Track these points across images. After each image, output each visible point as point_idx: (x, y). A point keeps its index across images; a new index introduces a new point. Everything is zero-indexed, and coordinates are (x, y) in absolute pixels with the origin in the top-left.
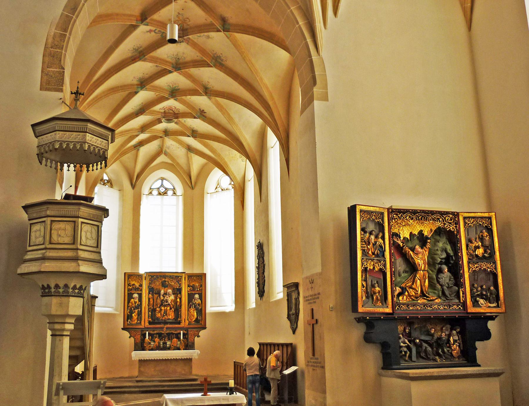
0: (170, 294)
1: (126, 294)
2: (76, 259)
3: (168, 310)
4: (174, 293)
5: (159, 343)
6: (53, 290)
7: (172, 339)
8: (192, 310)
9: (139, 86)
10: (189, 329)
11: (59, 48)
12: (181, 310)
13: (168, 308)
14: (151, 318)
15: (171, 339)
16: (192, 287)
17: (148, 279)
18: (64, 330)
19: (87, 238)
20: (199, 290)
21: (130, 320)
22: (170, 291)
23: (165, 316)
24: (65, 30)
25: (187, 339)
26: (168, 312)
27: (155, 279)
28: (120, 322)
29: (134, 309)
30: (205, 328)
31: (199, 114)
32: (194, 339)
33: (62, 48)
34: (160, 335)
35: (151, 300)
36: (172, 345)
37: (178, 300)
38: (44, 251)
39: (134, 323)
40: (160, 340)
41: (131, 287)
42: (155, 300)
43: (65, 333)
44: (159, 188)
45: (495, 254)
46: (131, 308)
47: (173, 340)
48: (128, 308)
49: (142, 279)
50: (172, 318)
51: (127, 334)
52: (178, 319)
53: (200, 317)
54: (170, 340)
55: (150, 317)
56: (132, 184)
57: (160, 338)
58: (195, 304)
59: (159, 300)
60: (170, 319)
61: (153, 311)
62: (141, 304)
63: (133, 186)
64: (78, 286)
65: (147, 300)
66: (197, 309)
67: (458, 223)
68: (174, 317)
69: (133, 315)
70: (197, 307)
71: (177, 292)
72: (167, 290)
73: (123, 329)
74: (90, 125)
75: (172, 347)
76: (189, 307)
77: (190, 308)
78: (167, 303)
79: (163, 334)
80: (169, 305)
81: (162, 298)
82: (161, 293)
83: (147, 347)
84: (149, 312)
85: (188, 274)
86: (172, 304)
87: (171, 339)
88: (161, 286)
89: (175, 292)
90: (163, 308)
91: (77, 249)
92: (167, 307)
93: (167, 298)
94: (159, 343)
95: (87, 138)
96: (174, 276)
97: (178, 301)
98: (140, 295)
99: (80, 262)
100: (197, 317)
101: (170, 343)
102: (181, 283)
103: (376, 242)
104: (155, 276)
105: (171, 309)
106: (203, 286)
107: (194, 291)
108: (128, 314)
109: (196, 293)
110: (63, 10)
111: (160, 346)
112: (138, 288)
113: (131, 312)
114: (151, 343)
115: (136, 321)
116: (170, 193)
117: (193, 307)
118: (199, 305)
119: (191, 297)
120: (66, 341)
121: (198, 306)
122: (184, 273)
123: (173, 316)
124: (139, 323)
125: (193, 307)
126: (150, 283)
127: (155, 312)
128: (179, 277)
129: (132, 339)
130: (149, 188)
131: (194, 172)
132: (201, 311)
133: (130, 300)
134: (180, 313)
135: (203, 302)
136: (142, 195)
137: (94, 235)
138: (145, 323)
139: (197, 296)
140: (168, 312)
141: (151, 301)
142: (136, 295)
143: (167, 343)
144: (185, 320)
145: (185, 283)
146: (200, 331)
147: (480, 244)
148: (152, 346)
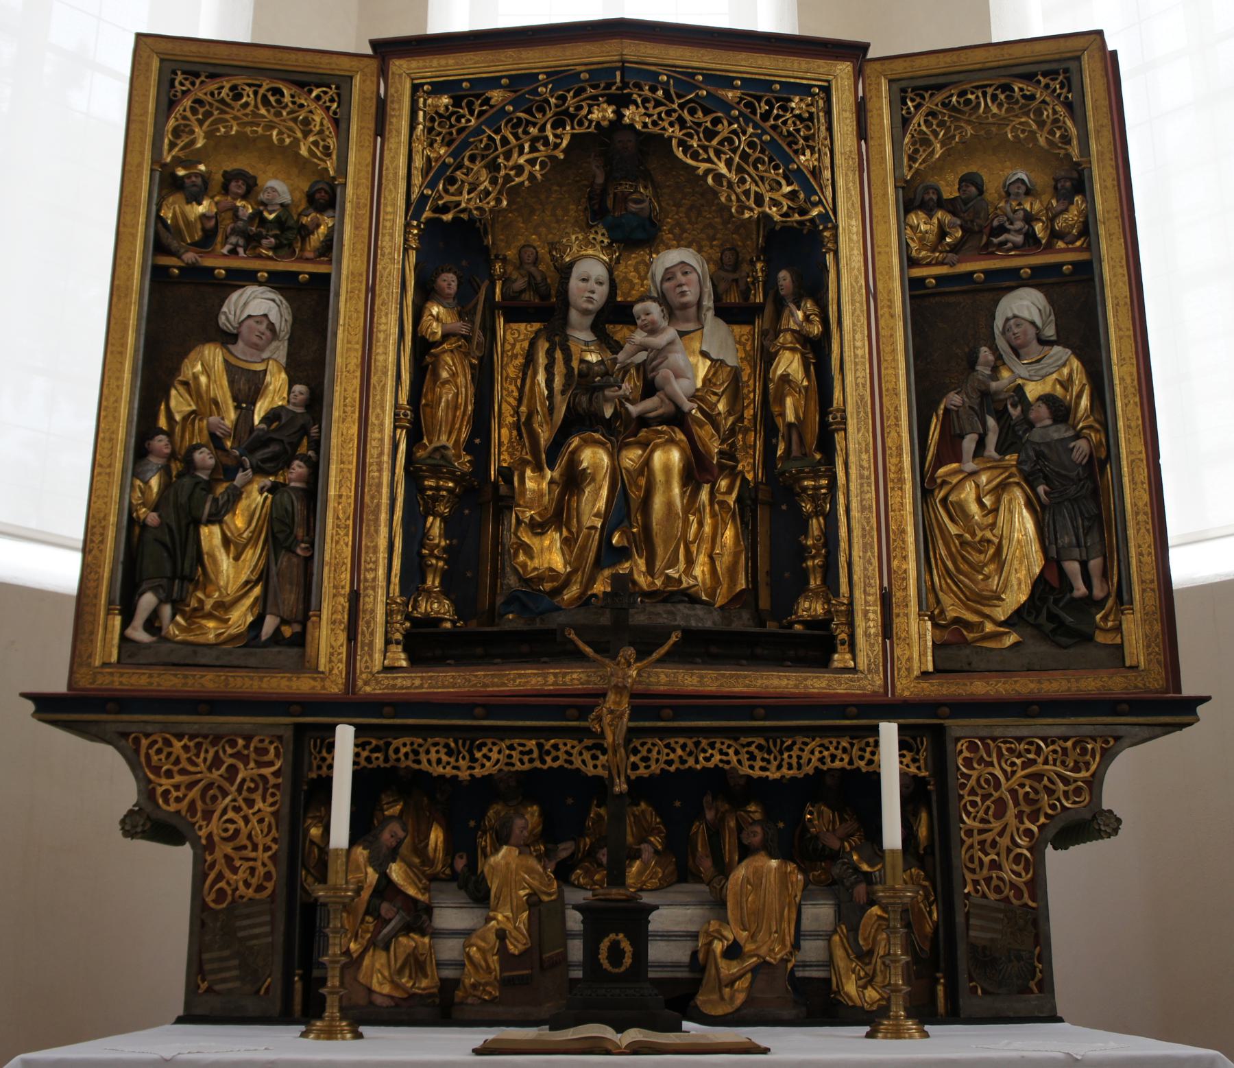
0: (691, 297)
3: (659, 476)
4: (733, 298)
7: (724, 870)
10: (956, 726)
12: (833, 485)
13: (658, 458)
14: (447, 590)
15: (706, 865)
16: (950, 206)
17: (412, 128)
20: (1055, 235)
23: (623, 554)
26: (658, 502)
36: (718, 946)
37: (790, 364)
39: (211, 637)
40: (563, 873)
41: (201, 209)
47: (741, 872)
48: (141, 452)
49: (340, 123)
50: (720, 601)
52: (790, 608)
53: (1095, 564)
54: (698, 879)
55: (433, 582)
57: (565, 850)
58: (1015, 412)
59: (549, 369)
60: (690, 597)
62: (316, 404)
68: (742, 584)
69: (211, 536)
70: (1036, 435)
75: (729, 969)
77: (950, 450)
79: (598, 788)
80: (678, 418)
82: (574, 284)
85: (899, 68)
86: (712, 419)
87: (706, 865)
89: (745, 294)
90: (594, 457)
92: (644, 445)
96: (727, 82)
97: (785, 378)
100: (1053, 562)
101: (690, 912)
102: (816, 172)
104: (494, 82)
107: (987, 251)
108: (144, 526)
109: (1008, 280)
111: (562, 960)
114: (429, 910)
115: (240, 617)
117: (992, 440)
118: (1060, 410)
121: (1045, 428)
123: (732, 571)
124: (277, 636)
125: (992, 440)
126: (439, 174)
127: (498, 520)
133: (184, 354)
134: (815, 525)
135: (1121, 372)
140: (669, 504)
141: (445, 375)
143: (659, 920)
144: (886, 599)
145: (862, 165)
146: (1108, 756)
148: (449, 949)
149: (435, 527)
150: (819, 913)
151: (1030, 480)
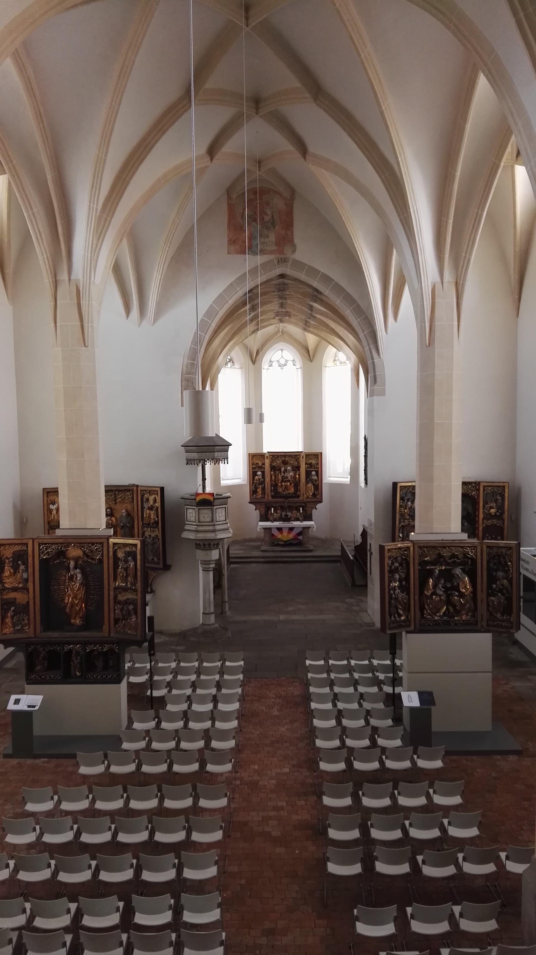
1: (251, 473)
2: (214, 531)
5: (281, 514)
6: (202, 547)
7: (292, 511)
8: (310, 485)
9: (251, 310)
11: (191, 374)
18: (210, 568)
19: (219, 517)
21: (256, 494)
22: (289, 468)
24: (194, 360)
25: (306, 512)
27: (276, 458)
28: (247, 491)
29: (259, 485)
30: (321, 502)
31: (309, 316)
32: (312, 512)
33: (193, 374)
34: (283, 508)
35: (273, 477)
37: (297, 476)
38: (196, 527)
40: (282, 511)
42: (277, 477)
43: (210, 569)
44: (278, 361)
45: (504, 513)
46: (256, 485)
48: (253, 484)
49: (264, 459)
51: (253, 507)
56: (252, 360)
61: (275, 486)
62: (264, 480)
63: (254, 362)
64: (216, 543)
65: (269, 477)
66: (314, 485)
67: (478, 490)
71: (297, 468)
72: (287, 467)
73: (249, 503)
74: (216, 447)
76: (307, 483)
77: (308, 483)
78: (287, 479)
80: (289, 480)
81: (283, 474)
83: (271, 518)
84: (271, 486)
88: (282, 465)
90: (283, 484)
91: (214, 525)
93: (287, 475)
94: (281, 514)
95: (216, 455)
98: (263, 473)
99: (217, 533)
103: (411, 507)
105: (291, 484)
106: (319, 464)
109: (313, 471)
110: (191, 344)
112: (261, 467)
113: (256, 488)
115: (260, 496)
116: (290, 363)
118: (316, 481)
119: (308, 474)
120: (211, 573)
122: (302, 452)
126: (272, 462)
128: (297, 456)
129: (257, 510)
130: (269, 361)
131: (311, 348)
132: (318, 486)
135: (320, 478)
136: (262, 369)
137: (224, 514)
138: (268, 498)
139: (314, 473)
142: (259, 473)
147: (495, 504)
149: (272, 488)
150: (298, 514)
151: (313, 486)
